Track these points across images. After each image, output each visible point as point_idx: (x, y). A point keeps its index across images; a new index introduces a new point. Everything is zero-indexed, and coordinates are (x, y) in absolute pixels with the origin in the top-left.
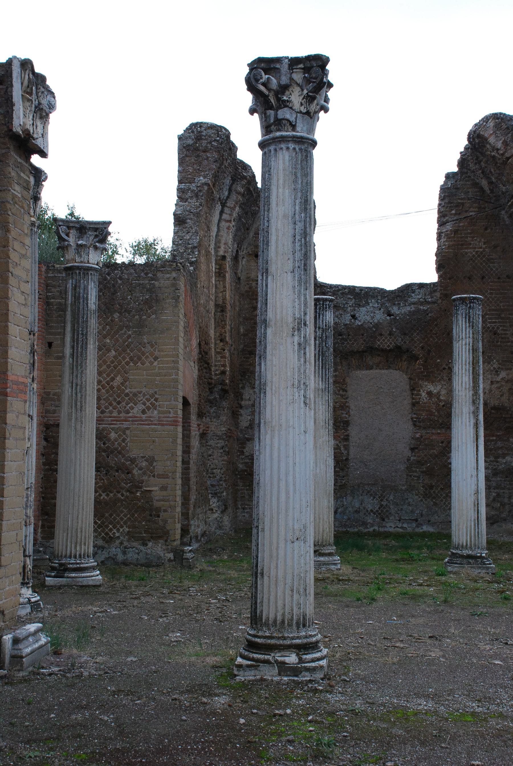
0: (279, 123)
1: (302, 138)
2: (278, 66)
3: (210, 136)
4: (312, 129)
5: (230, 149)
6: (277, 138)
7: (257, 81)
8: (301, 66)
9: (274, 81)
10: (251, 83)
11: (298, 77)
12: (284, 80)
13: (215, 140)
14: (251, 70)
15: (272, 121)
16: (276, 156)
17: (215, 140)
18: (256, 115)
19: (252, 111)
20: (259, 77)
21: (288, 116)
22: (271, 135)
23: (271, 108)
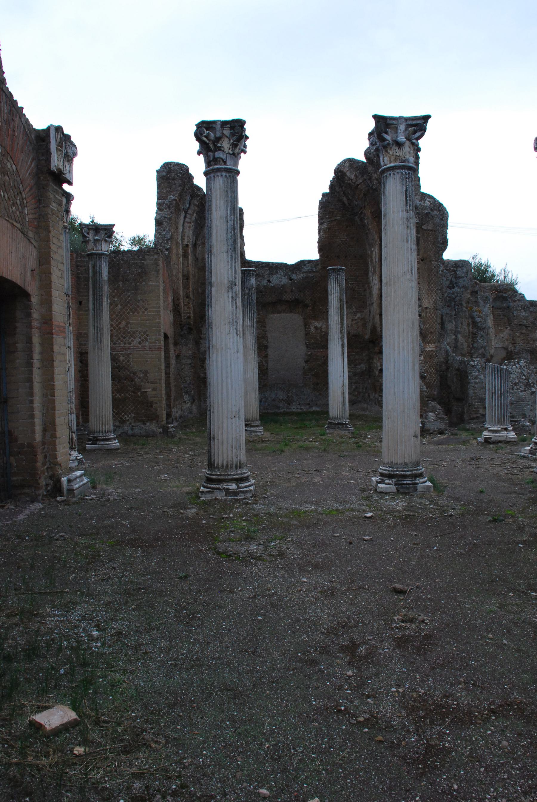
0: (216, 160)
1: (230, 169)
2: (214, 126)
3: (176, 170)
4: (236, 164)
5: (189, 178)
6: (215, 169)
7: (201, 134)
8: (229, 126)
9: (212, 134)
10: (198, 136)
11: (227, 132)
12: (218, 134)
13: (180, 173)
14: (198, 128)
15: (211, 159)
16: (214, 180)
17: (180, 173)
18: (202, 156)
19: (199, 153)
20: (202, 132)
21: (221, 156)
22: (211, 168)
23: (211, 151)
